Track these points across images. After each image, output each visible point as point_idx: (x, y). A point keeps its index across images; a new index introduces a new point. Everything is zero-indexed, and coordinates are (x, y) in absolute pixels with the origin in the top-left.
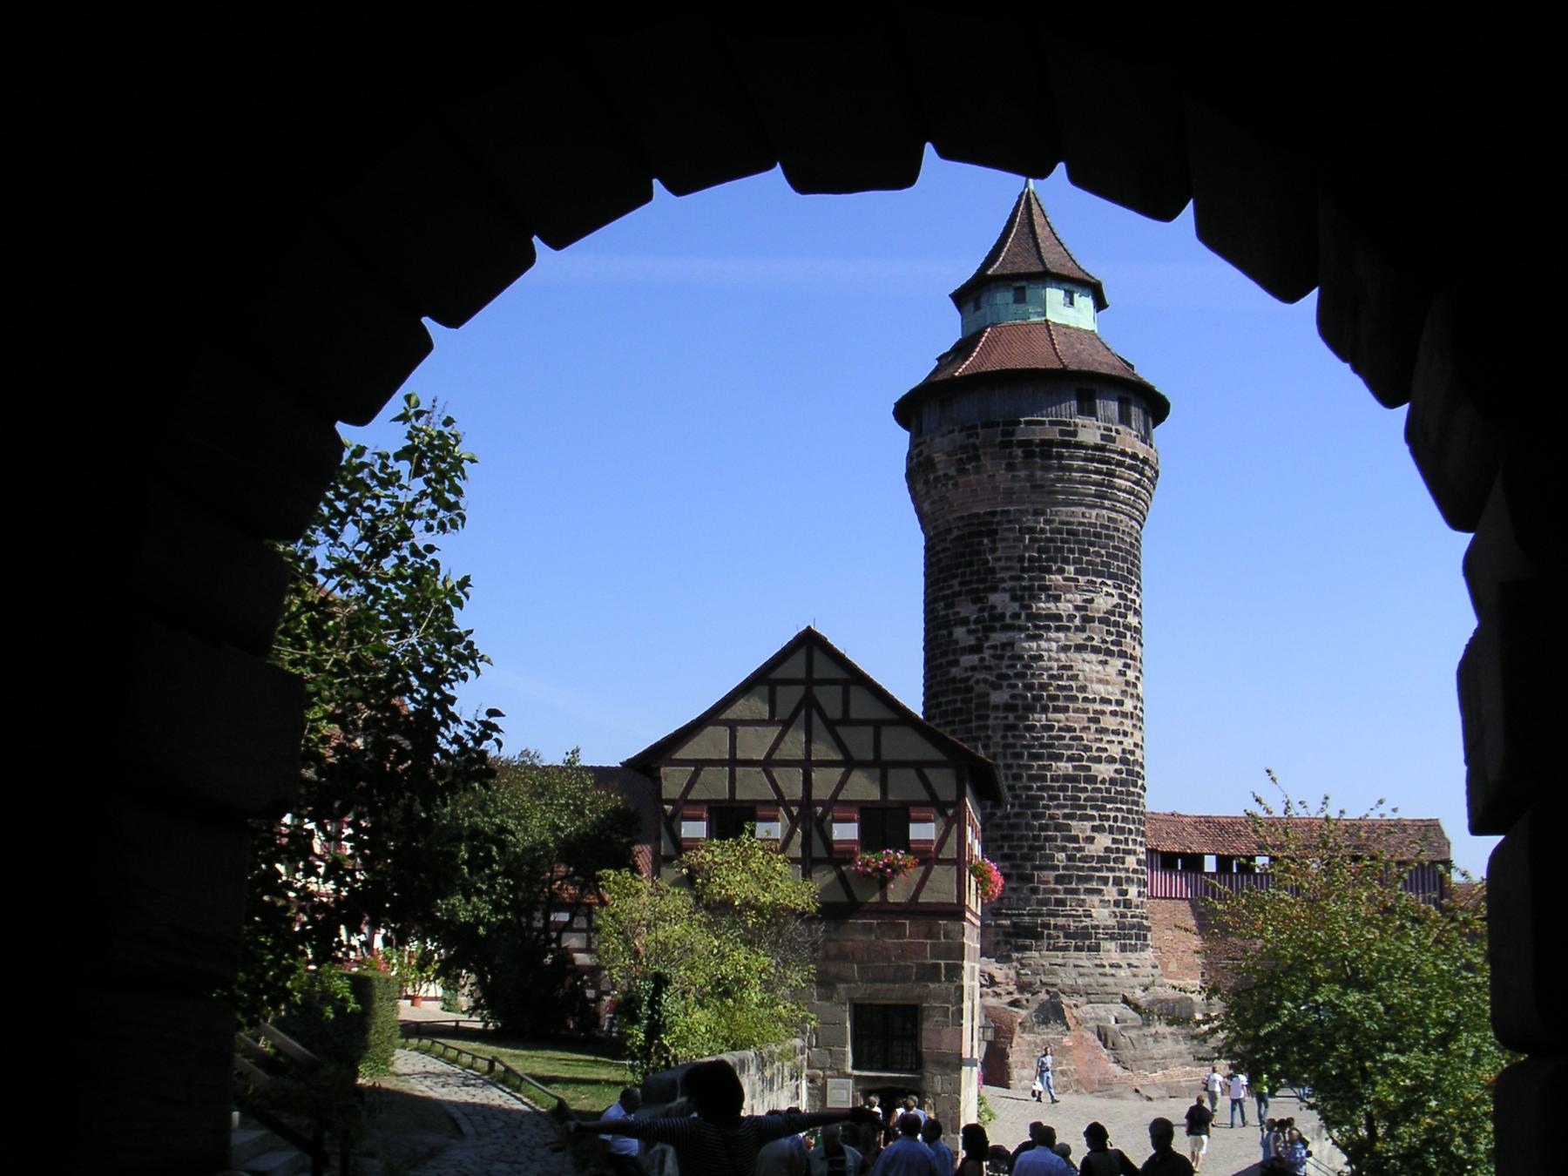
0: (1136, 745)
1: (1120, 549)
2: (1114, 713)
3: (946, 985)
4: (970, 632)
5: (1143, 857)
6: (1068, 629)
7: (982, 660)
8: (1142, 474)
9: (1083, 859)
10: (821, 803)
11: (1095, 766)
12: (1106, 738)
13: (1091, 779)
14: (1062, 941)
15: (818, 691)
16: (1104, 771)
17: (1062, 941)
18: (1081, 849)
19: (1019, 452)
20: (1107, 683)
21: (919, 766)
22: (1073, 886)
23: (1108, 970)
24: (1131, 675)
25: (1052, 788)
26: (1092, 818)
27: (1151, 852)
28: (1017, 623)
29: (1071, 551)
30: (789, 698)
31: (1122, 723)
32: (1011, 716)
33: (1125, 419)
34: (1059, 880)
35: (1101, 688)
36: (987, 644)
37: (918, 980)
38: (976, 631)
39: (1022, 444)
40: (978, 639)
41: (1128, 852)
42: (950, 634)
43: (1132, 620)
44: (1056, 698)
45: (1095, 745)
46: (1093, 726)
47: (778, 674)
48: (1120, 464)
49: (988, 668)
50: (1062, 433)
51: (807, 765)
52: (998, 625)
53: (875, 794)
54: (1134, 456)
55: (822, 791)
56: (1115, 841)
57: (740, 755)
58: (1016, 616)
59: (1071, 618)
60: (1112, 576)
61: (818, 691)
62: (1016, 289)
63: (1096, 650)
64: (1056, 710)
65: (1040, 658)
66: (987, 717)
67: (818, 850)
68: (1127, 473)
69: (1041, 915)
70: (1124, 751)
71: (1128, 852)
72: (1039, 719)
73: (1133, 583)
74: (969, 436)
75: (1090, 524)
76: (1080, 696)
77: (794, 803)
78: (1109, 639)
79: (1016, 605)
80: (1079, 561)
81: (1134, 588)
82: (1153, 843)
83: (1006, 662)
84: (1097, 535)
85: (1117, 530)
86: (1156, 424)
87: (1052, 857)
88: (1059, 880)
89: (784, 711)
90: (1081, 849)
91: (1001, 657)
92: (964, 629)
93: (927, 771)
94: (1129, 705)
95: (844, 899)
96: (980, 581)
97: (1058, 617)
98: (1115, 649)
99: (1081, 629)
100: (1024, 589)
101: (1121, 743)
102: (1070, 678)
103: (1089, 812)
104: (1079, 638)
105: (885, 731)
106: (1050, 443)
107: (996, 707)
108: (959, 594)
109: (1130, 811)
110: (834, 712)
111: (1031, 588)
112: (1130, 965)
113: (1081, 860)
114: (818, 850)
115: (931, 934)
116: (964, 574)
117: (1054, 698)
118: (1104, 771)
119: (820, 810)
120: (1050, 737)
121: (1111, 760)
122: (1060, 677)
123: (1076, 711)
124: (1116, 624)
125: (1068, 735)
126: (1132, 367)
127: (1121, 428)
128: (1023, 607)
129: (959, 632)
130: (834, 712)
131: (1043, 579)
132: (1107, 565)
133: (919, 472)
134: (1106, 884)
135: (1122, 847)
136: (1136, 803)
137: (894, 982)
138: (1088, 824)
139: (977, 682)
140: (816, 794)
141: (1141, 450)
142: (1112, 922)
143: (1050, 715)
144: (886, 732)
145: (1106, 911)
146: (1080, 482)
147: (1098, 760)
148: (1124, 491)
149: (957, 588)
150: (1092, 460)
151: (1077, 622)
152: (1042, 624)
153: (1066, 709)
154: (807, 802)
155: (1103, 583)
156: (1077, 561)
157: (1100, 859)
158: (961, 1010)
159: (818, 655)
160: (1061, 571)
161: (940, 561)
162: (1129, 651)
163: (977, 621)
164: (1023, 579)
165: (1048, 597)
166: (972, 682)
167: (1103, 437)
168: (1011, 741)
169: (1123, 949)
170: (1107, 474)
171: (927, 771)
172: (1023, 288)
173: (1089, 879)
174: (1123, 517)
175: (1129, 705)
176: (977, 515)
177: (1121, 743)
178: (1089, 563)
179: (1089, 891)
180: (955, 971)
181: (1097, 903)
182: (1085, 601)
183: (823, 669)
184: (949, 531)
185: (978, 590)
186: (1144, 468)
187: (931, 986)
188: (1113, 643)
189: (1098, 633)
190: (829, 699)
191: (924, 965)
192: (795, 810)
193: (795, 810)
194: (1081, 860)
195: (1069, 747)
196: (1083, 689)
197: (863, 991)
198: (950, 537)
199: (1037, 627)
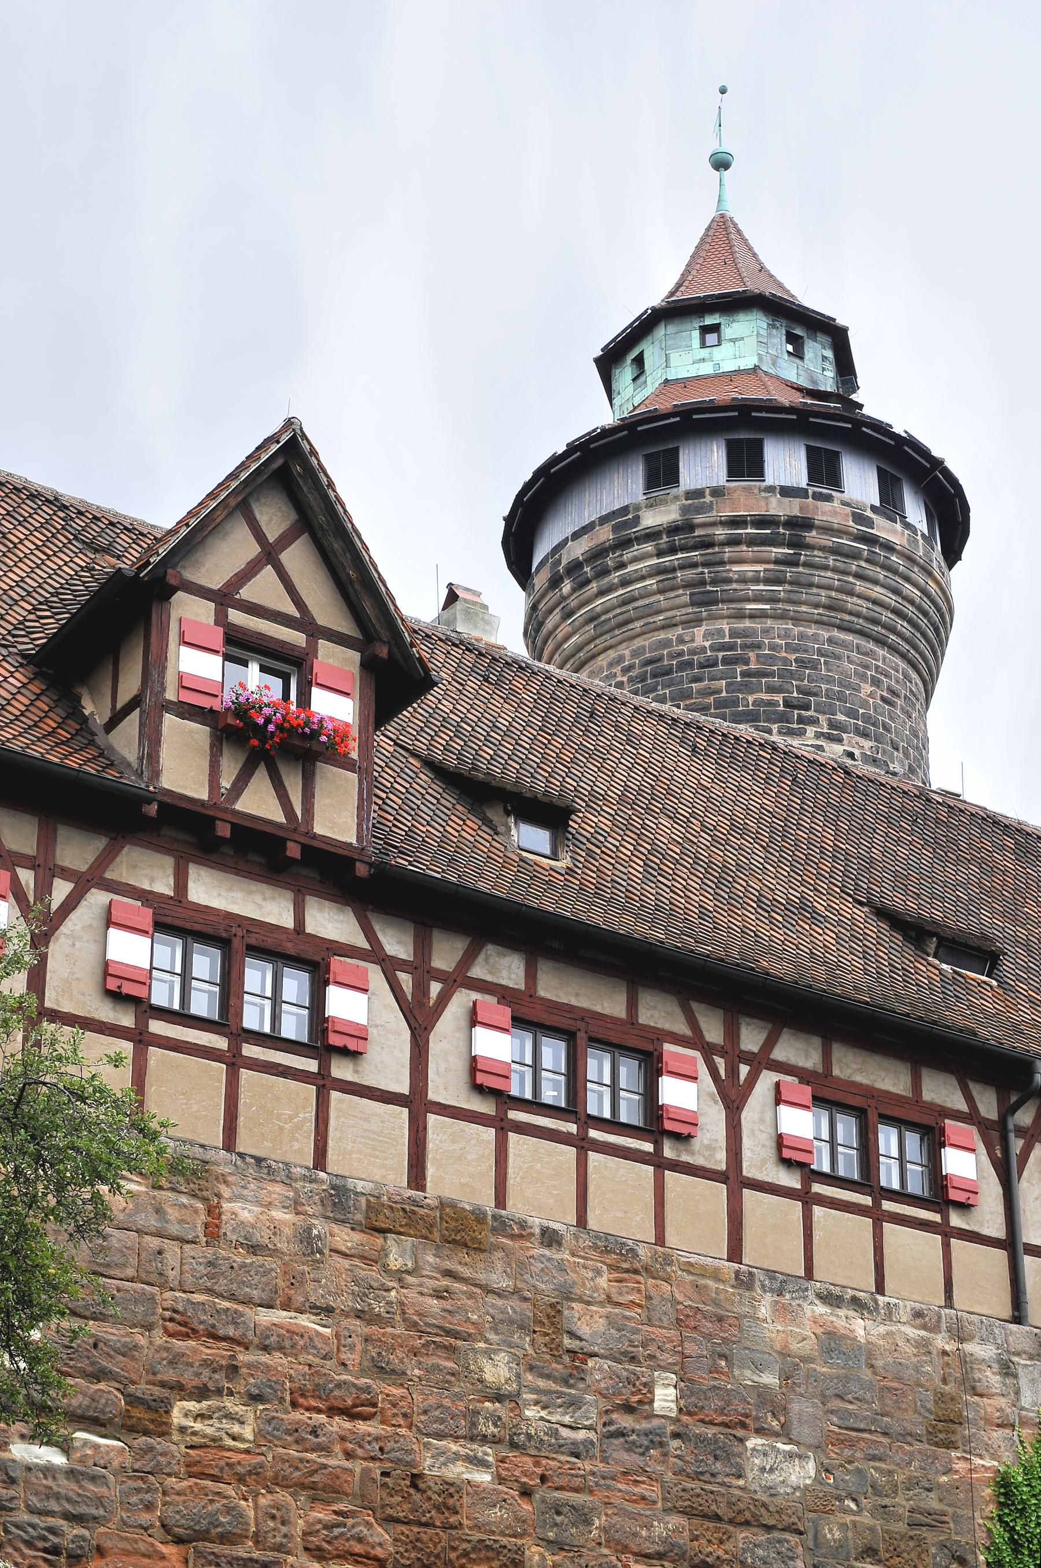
8: (797, 544)
39: (575, 567)
54: (761, 522)
75: (693, 652)
84: (712, 663)
85: (759, 646)
146: (661, 592)
148: (756, 580)
150: (673, 550)
170: (705, 565)
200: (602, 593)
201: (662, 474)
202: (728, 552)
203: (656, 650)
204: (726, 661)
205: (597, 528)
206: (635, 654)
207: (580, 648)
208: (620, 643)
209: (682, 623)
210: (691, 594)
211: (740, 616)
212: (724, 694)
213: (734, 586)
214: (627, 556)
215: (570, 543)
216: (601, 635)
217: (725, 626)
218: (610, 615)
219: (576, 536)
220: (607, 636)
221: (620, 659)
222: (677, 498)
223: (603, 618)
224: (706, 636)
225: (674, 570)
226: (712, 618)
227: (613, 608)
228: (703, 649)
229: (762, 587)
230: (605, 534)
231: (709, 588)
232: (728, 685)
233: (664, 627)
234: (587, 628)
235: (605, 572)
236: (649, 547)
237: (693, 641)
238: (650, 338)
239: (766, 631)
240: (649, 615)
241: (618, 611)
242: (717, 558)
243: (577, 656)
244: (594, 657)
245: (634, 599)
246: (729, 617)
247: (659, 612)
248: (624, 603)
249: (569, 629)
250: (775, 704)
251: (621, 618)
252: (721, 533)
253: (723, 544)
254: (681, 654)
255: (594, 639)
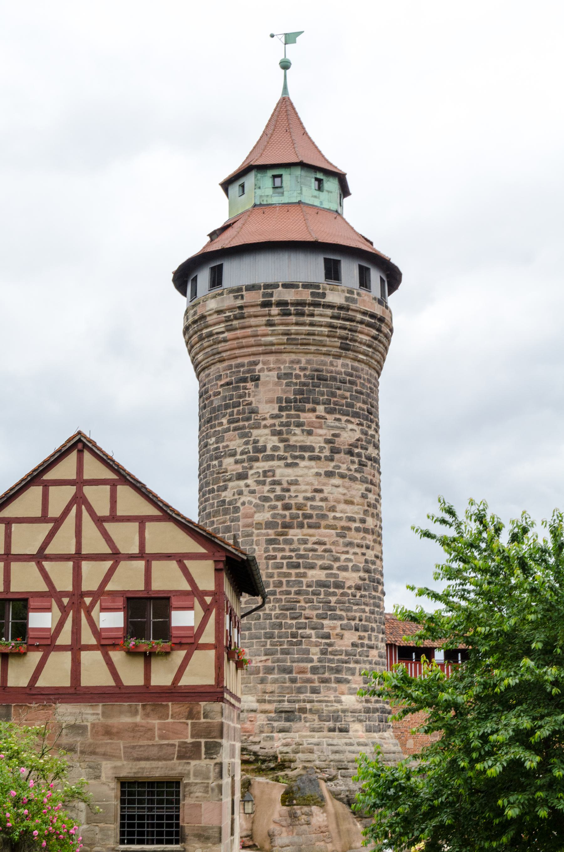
0: (377, 557)
1: (361, 393)
2: (358, 530)
3: (208, 761)
4: (237, 462)
5: (383, 651)
6: (319, 458)
7: (247, 486)
8: (379, 330)
9: (333, 653)
10: (89, 593)
11: (343, 575)
12: (352, 551)
13: (338, 585)
14: (317, 724)
15: (88, 491)
16: (351, 578)
17: (317, 724)
18: (330, 645)
19: (275, 310)
20: (352, 503)
21: (180, 558)
22: (327, 675)
23: (355, 748)
24: (371, 497)
25: (307, 593)
26: (341, 618)
27: (390, 646)
28: (276, 454)
29: (323, 395)
30: (60, 497)
31: (363, 538)
32: (270, 531)
33: (364, 282)
34: (314, 670)
35: (348, 508)
36: (251, 472)
37: (180, 757)
38: (242, 461)
39: (281, 304)
40: (243, 468)
41: (371, 647)
42: (220, 465)
43: (371, 451)
44: (310, 517)
45: (343, 557)
46: (341, 540)
47: (49, 476)
48: (362, 322)
49: (253, 492)
50: (313, 294)
51: (78, 558)
52: (260, 456)
53: (137, 585)
54: (373, 316)
55: (90, 583)
56: (361, 638)
57: (14, 550)
58: (275, 448)
59: (322, 449)
60: (356, 415)
61: (88, 491)
62: (274, 177)
63: (342, 476)
64: (310, 527)
65: (296, 483)
66: (251, 535)
67: (88, 638)
68: (367, 329)
69: (299, 701)
70: (366, 561)
71: (371, 647)
72: (295, 534)
73: (372, 421)
74: (236, 298)
76: (331, 515)
77: (65, 594)
78: (353, 467)
79: (275, 438)
80: (328, 402)
81: (374, 426)
82: (391, 640)
83: (267, 488)
85: (360, 377)
86: (390, 293)
87: (307, 652)
88: (314, 670)
89: (55, 511)
90: (330, 645)
91: (263, 483)
92: (231, 460)
93: (188, 563)
94: (370, 522)
95: (111, 682)
96: (243, 420)
97: (311, 449)
98: (358, 475)
99: (332, 460)
100: (282, 424)
101: (364, 554)
102: (322, 500)
103: (338, 612)
104: (330, 467)
105: (149, 526)
106: (302, 303)
107: (259, 526)
108: (228, 430)
109: (372, 612)
110: (103, 510)
111: (288, 425)
112: (374, 744)
113: (332, 653)
114: (88, 638)
115: (191, 715)
116: (232, 414)
117: (306, 516)
118: (351, 578)
119: (88, 600)
120: (305, 550)
121: (356, 569)
122: (313, 499)
123: (328, 527)
124: (359, 455)
125: (320, 548)
126: (371, 243)
127: (363, 292)
128: (282, 441)
129: (228, 462)
130: (103, 510)
131: (298, 417)
132: (351, 406)
133: (196, 330)
134: (353, 674)
135: (366, 642)
136: (378, 606)
137: (159, 759)
138: (339, 623)
139: (243, 504)
140: (86, 587)
141: (378, 310)
142: (359, 706)
143: (306, 531)
144: (149, 526)
145: (353, 698)
146: (328, 336)
147: (344, 569)
148: (365, 344)
149: (226, 426)
150: (338, 318)
151: (327, 453)
152: (297, 454)
153: (317, 526)
154: (77, 595)
155: (348, 421)
156: (328, 402)
157: (347, 654)
158: (220, 787)
159: (87, 455)
160: (314, 410)
161: (212, 402)
162: (370, 477)
163: (242, 453)
164: (281, 417)
165: (303, 431)
166: (239, 504)
167: (347, 299)
168: (272, 553)
169: (369, 730)
170: (350, 330)
171: (188, 563)
172: (280, 176)
173: (338, 671)
174: (363, 366)
175: (370, 522)
176: (243, 365)
177: (364, 554)
178: (336, 404)
179: (339, 681)
180: (213, 749)
181: (346, 691)
182: (334, 435)
183: (93, 469)
184: (219, 378)
185: (244, 427)
186: (381, 327)
187: (193, 763)
188: (356, 471)
189: (344, 463)
190: (98, 498)
191: (186, 743)
192: (66, 601)
193: (66, 601)
194: (332, 653)
195: (322, 557)
196: (333, 509)
197: (129, 769)
198: (220, 383)
199: (295, 457)
200: (297, 324)
201: (333, 272)
202: (360, 327)
203: (319, 365)
204: (351, 383)
205: (300, 289)
206: (308, 362)
207: (273, 344)
208: (300, 353)
209: (333, 355)
210: (341, 343)
211: (355, 359)
212: (349, 400)
213: (357, 344)
214: (318, 311)
215: (280, 288)
216: (290, 344)
217: (349, 362)
218: (299, 337)
219: (286, 286)
220: (295, 347)
221: (299, 362)
222: (343, 291)
223: (293, 336)
224: (343, 365)
225: (336, 328)
226: (346, 357)
227: (301, 334)
228: (340, 373)
229: (365, 348)
230: (306, 295)
231: (348, 342)
232: (351, 395)
233: (324, 354)
234: (281, 337)
235: (302, 314)
236: (329, 312)
237: (337, 366)
238: (288, 171)
239: (362, 370)
240: (319, 345)
241: (303, 337)
242: (353, 328)
243: (270, 348)
244: (281, 353)
245: (314, 334)
246: (352, 359)
247: (324, 346)
248: (309, 334)
249: (270, 332)
250: (363, 410)
251: (305, 341)
252: (359, 317)
253: (358, 322)
254: (332, 372)
255: (284, 344)
